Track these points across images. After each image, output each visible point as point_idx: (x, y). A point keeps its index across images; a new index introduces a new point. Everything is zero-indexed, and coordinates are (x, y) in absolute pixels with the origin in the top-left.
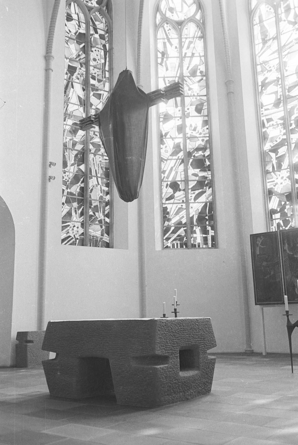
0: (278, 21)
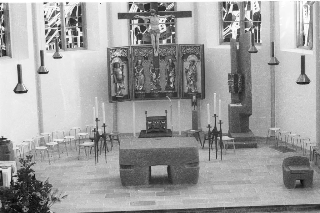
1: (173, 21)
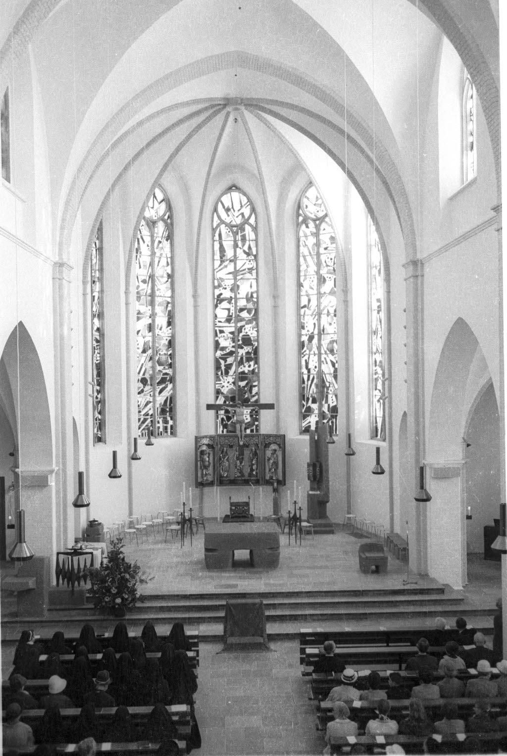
0: (236, 246)
1: (257, 412)
